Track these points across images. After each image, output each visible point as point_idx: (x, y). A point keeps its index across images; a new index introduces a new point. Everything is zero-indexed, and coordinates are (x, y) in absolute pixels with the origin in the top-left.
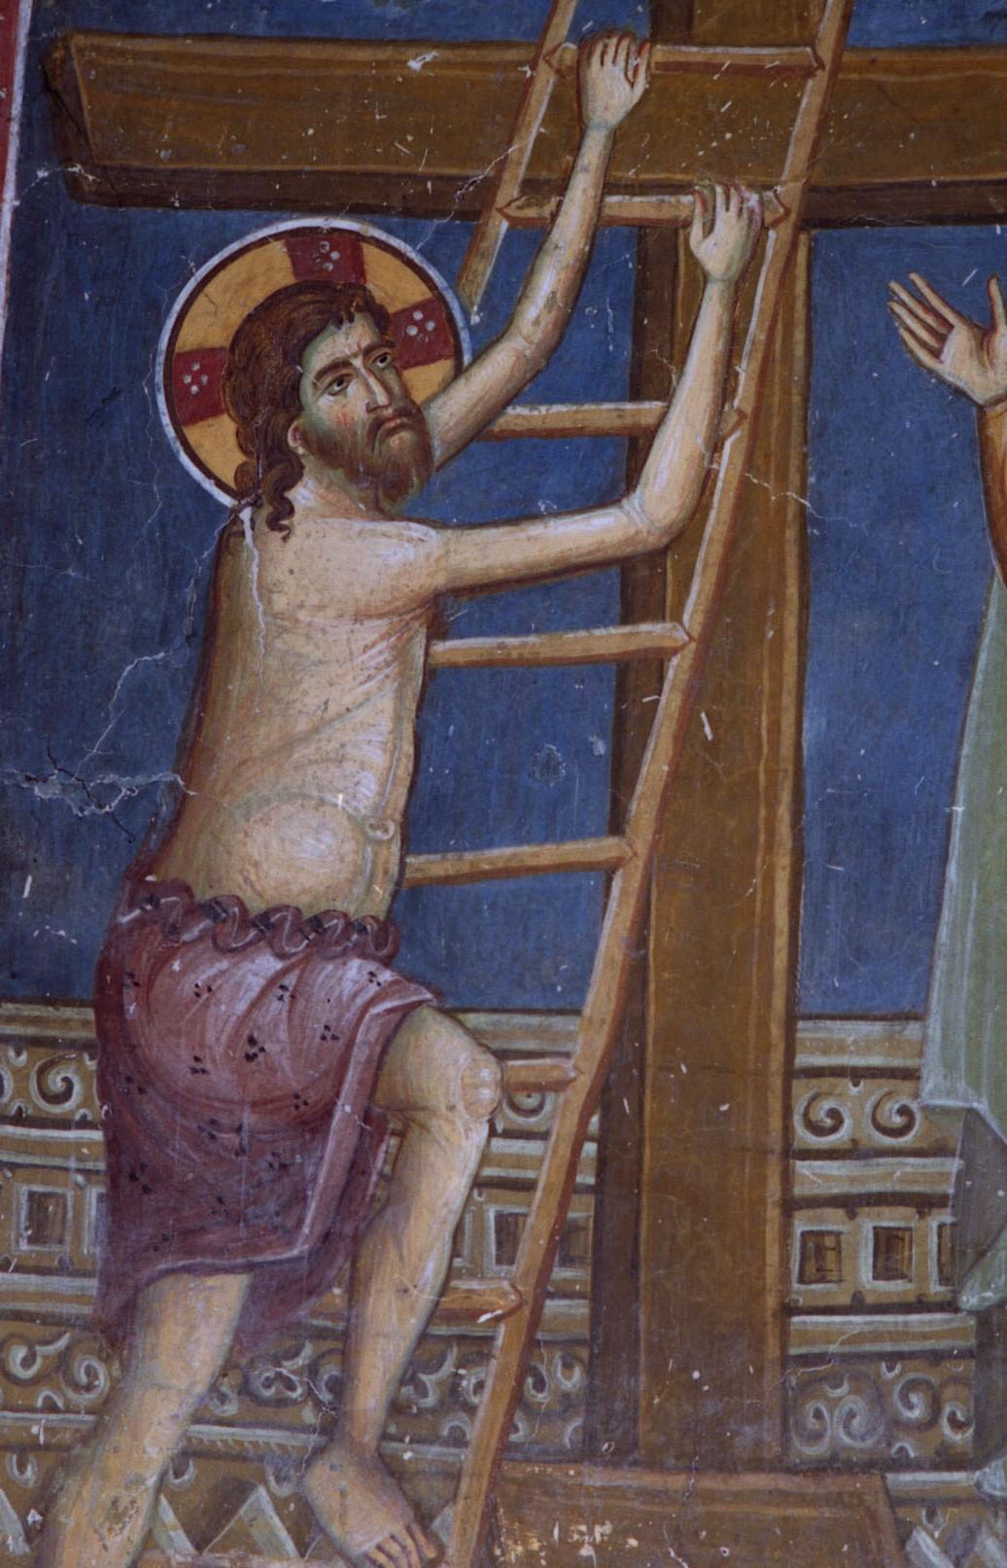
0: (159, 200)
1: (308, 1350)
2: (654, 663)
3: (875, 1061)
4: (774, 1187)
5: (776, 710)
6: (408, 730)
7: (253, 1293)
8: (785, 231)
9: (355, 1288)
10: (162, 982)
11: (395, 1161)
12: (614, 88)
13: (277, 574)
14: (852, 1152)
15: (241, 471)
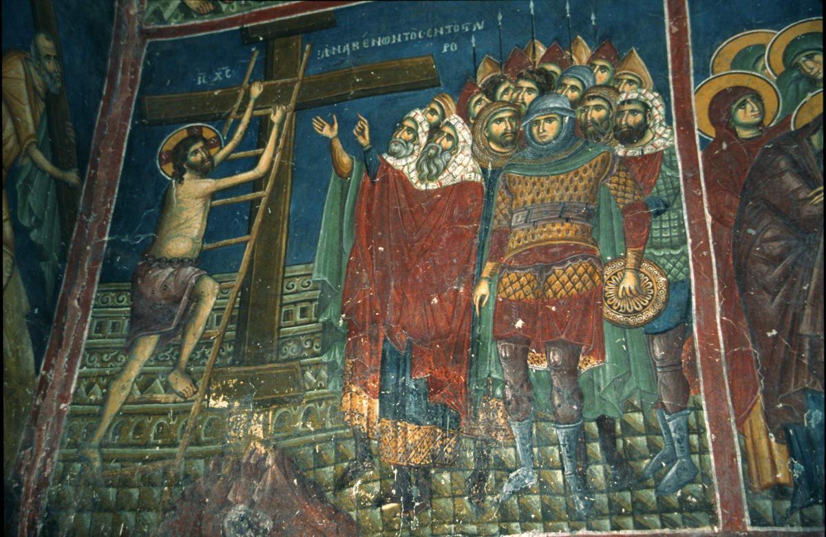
0: (161, 124)
1: (172, 349)
2: (259, 200)
3: (303, 273)
4: (278, 302)
5: (285, 205)
6: (206, 219)
7: (161, 337)
8: (291, 112)
9: (184, 336)
10: (146, 277)
11: (195, 307)
12: (256, 90)
13: (180, 192)
14: (297, 292)
15: (173, 173)
